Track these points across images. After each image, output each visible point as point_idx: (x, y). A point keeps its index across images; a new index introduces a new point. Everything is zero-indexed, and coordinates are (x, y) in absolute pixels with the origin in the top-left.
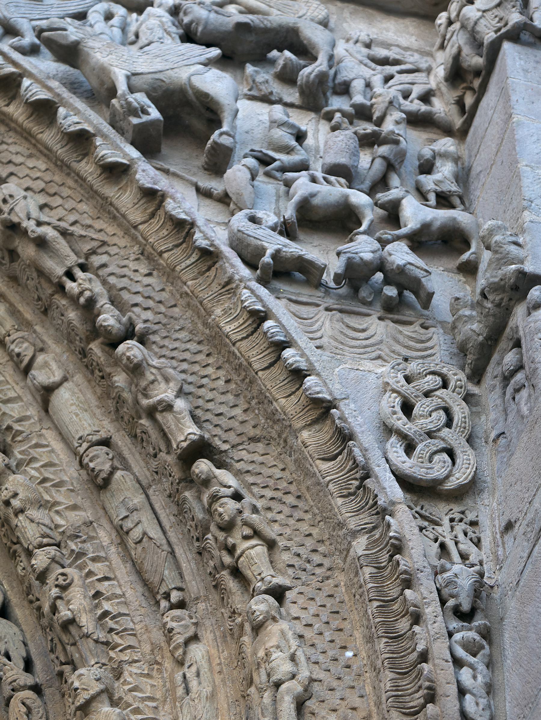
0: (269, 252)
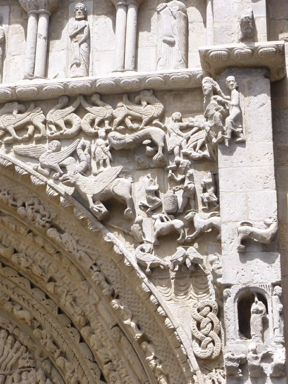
0: (148, 266)
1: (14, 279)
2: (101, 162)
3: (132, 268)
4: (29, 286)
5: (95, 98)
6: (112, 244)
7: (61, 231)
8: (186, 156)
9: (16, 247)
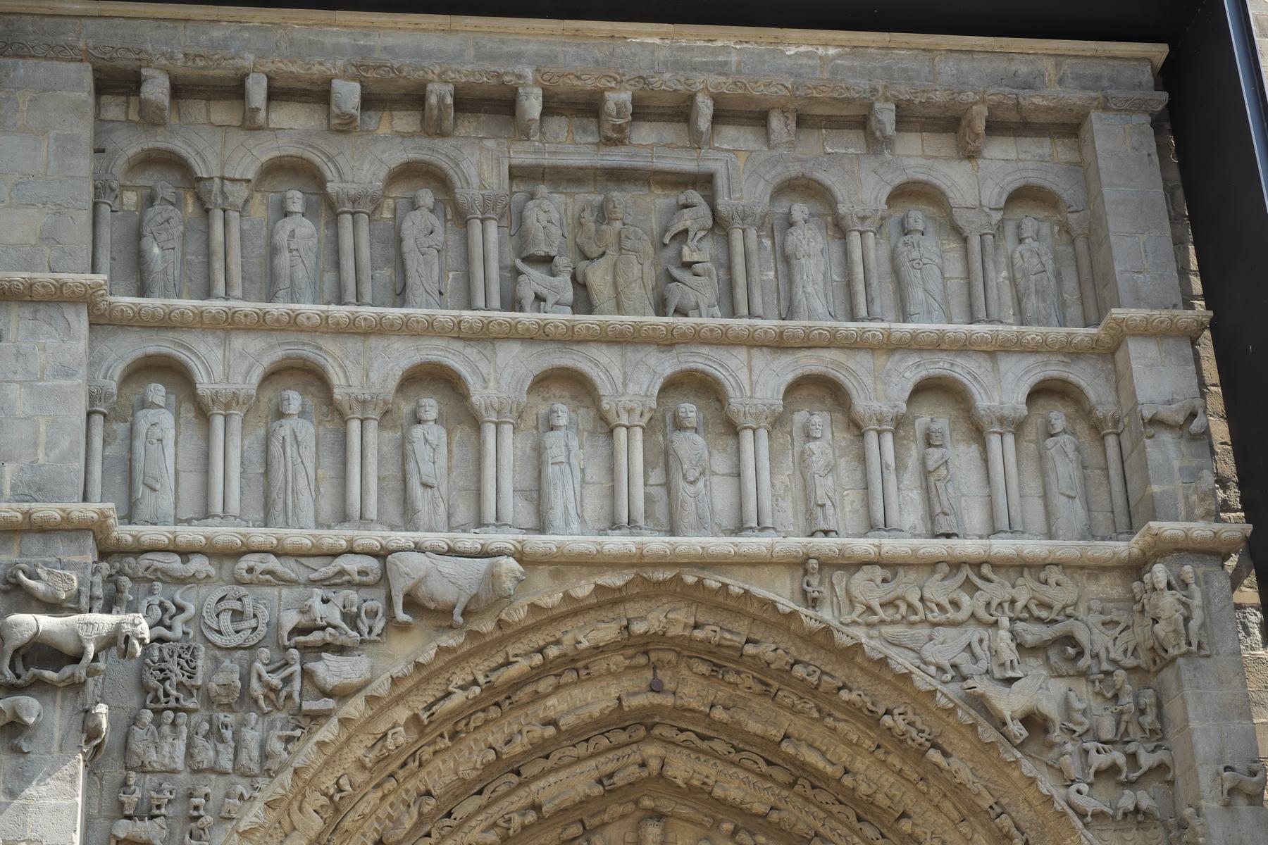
0: (1090, 814)
1: (829, 807)
2: (1008, 663)
3: (1064, 814)
4: (855, 819)
5: (986, 570)
6: (1032, 781)
7: (945, 754)
8: (1113, 662)
9: (847, 764)
